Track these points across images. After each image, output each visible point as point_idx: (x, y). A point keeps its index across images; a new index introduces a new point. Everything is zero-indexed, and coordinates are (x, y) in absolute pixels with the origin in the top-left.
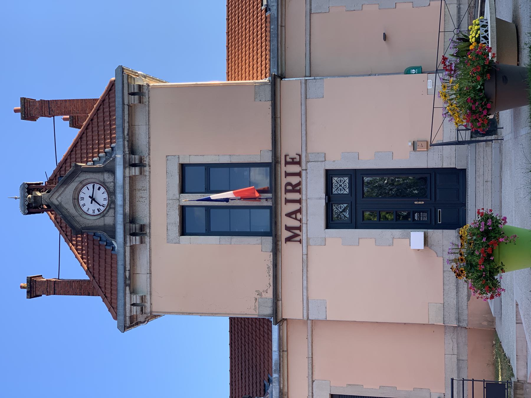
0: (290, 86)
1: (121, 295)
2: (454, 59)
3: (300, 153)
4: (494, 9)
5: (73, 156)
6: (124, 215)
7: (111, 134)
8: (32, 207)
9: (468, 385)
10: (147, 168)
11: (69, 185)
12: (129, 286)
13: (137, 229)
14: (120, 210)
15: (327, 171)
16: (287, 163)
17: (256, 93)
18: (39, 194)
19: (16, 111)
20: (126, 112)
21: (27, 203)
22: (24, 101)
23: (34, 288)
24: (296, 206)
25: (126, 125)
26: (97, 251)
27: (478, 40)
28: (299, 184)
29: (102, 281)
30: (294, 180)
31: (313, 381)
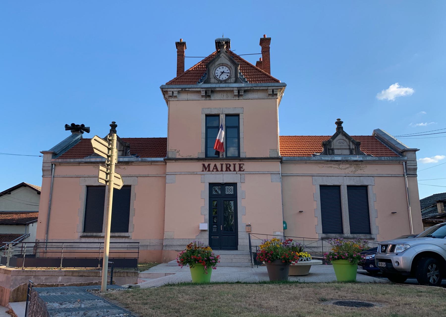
0: (277, 167)
1: (178, 86)
2: (291, 245)
4: (315, 264)
5: (243, 63)
6: (215, 88)
7: (254, 81)
8: (219, 44)
10: (237, 98)
11: (229, 61)
12: (182, 90)
13: (208, 94)
14: (217, 85)
15: (236, 184)
16: (240, 164)
17: (273, 150)
18: (225, 47)
19: (264, 36)
20: (264, 88)
21: (221, 41)
22: (269, 39)
24: (219, 169)
25: (258, 88)
26: (198, 75)
27: (300, 256)
29: (184, 78)
30: (232, 168)
31: (137, 177)
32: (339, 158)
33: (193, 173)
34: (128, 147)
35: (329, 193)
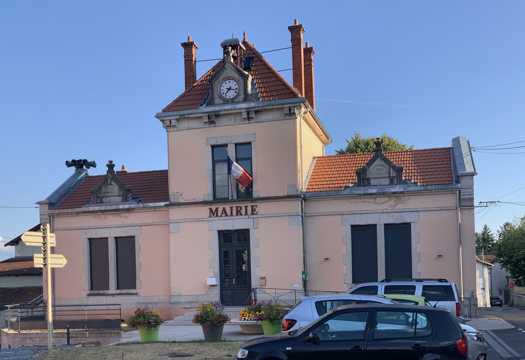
0: (296, 206)
1: (175, 113)
3: (258, 214)
6: (220, 111)
9: (118, 312)
10: (247, 122)
11: (237, 73)
12: (180, 118)
13: (212, 119)
14: (222, 108)
16: (252, 206)
17: (292, 185)
20: (278, 107)
23: (188, 46)
24: (229, 213)
25: (271, 107)
28: (241, 214)
30: (243, 211)
32: (374, 191)
33: (198, 220)
34: (129, 190)
35: (362, 235)
